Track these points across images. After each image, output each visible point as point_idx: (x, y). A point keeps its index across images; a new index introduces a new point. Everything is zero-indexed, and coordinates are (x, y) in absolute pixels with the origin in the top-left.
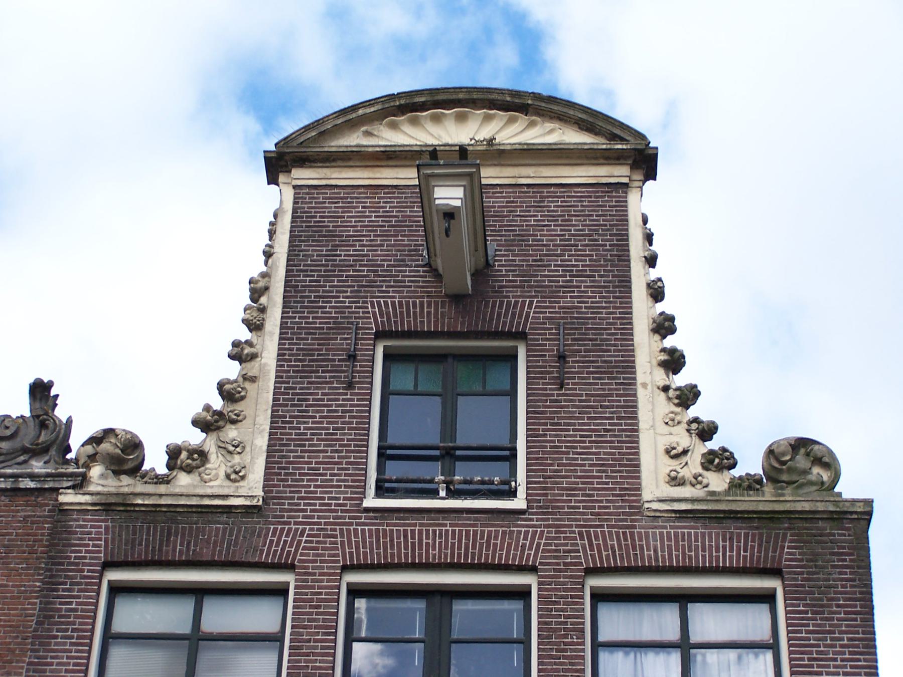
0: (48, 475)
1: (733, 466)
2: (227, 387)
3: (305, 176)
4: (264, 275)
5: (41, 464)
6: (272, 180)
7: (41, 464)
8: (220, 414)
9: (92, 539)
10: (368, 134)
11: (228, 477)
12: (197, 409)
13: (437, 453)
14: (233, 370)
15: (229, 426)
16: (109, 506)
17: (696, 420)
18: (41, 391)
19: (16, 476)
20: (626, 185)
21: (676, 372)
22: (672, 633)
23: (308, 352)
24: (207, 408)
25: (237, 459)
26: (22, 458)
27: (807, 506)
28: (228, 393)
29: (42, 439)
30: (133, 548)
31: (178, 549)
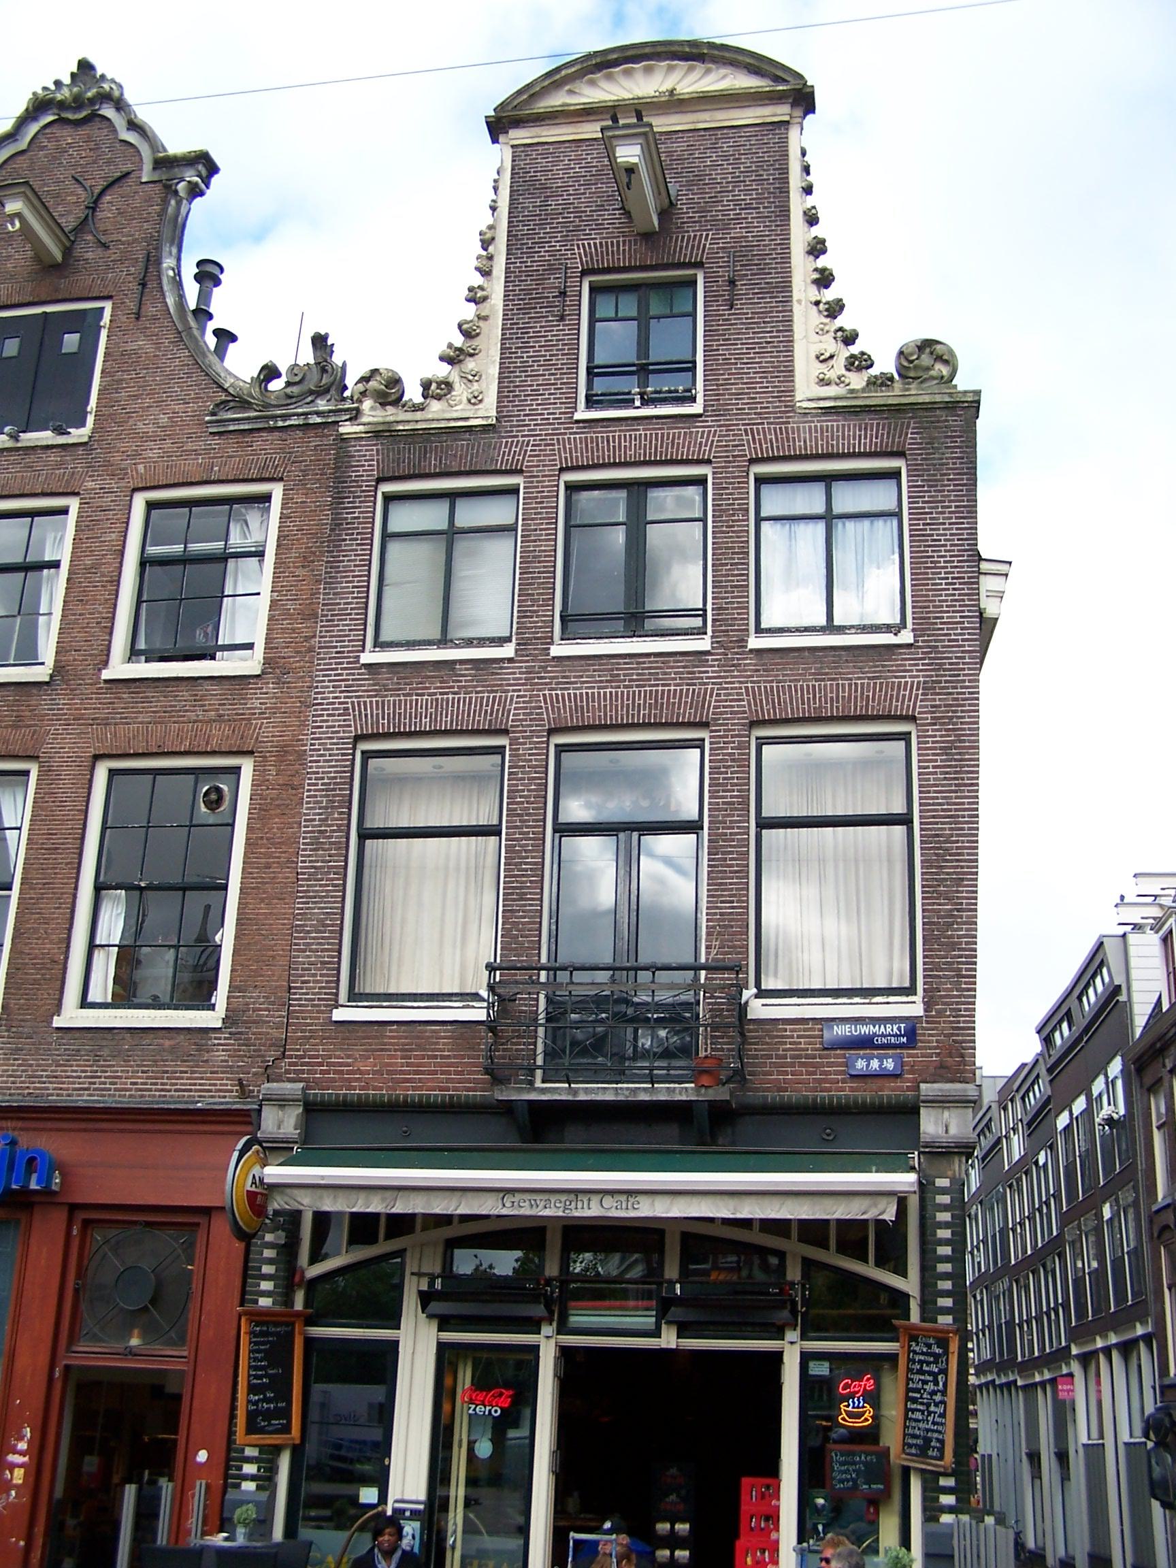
0: (330, 411)
1: (871, 366)
2: (465, 327)
3: (520, 136)
4: (491, 227)
5: (324, 402)
6: (495, 140)
7: (324, 402)
8: (460, 350)
9: (367, 459)
10: (571, 92)
11: (469, 401)
12: (442, 348)
13: (634, 368)
14: (469, 311)
15: (468, 359)
16: (381, 433)
17: (841, 329)
18: (320, 342)
19: (306, 414)
20: (788, 122)
21: (827, 287)
22: (820, 509)
23: (528, 292)
24: (450, 346)
25: (476, 386)
26: (310, 399)
27: (927, 399)
29: (324, 382)
30: (398, 465)
31: (433, 464)
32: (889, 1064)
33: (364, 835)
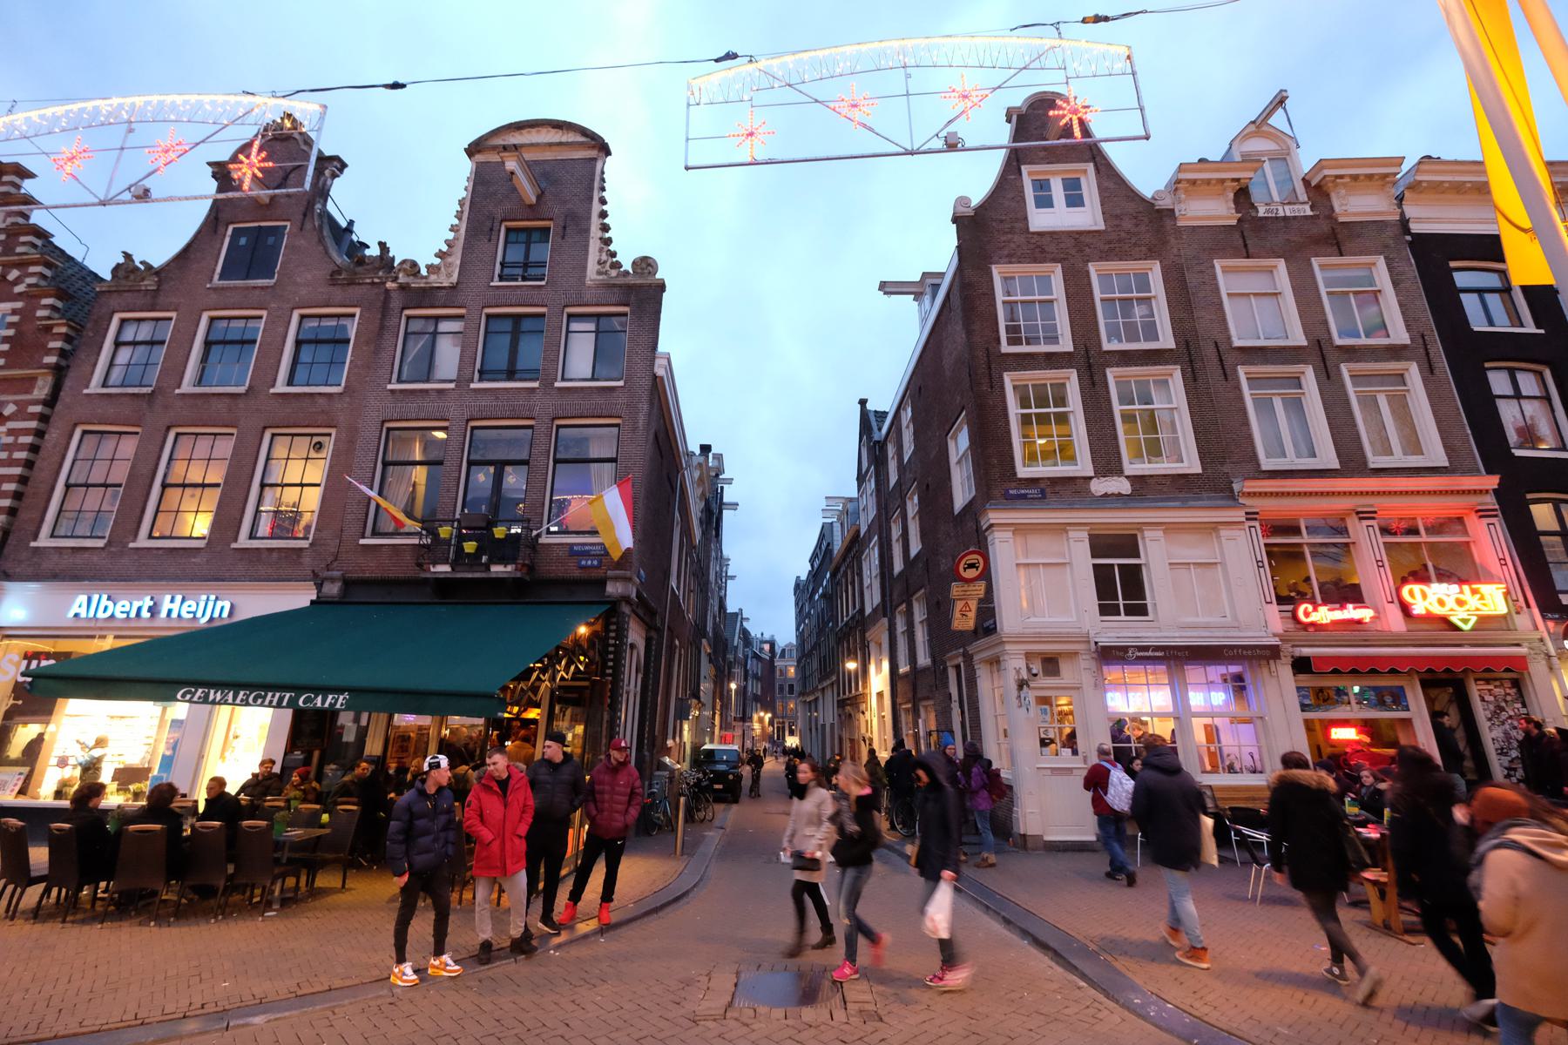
3: (479, 158)
16: (403, 288)
28: (449, 243)
33: (386, 464)
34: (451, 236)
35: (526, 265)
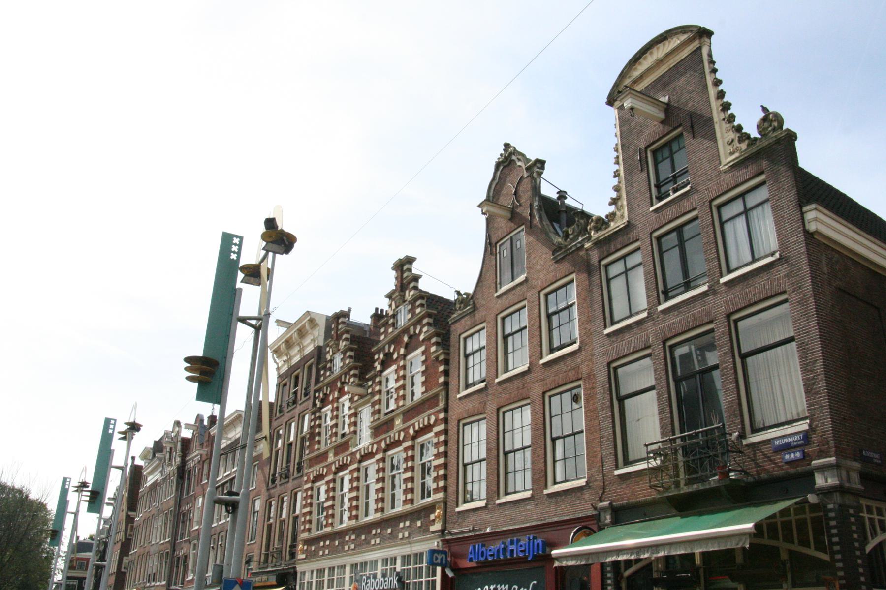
9: (594, 256)
28: (617, 189)
32: (798, 455)
34: (615, 182)
35: (675, 178)
